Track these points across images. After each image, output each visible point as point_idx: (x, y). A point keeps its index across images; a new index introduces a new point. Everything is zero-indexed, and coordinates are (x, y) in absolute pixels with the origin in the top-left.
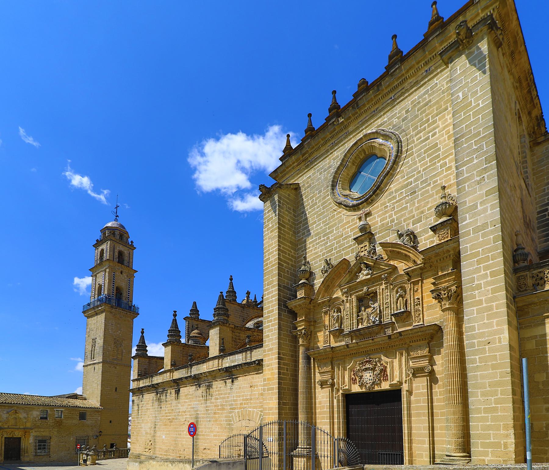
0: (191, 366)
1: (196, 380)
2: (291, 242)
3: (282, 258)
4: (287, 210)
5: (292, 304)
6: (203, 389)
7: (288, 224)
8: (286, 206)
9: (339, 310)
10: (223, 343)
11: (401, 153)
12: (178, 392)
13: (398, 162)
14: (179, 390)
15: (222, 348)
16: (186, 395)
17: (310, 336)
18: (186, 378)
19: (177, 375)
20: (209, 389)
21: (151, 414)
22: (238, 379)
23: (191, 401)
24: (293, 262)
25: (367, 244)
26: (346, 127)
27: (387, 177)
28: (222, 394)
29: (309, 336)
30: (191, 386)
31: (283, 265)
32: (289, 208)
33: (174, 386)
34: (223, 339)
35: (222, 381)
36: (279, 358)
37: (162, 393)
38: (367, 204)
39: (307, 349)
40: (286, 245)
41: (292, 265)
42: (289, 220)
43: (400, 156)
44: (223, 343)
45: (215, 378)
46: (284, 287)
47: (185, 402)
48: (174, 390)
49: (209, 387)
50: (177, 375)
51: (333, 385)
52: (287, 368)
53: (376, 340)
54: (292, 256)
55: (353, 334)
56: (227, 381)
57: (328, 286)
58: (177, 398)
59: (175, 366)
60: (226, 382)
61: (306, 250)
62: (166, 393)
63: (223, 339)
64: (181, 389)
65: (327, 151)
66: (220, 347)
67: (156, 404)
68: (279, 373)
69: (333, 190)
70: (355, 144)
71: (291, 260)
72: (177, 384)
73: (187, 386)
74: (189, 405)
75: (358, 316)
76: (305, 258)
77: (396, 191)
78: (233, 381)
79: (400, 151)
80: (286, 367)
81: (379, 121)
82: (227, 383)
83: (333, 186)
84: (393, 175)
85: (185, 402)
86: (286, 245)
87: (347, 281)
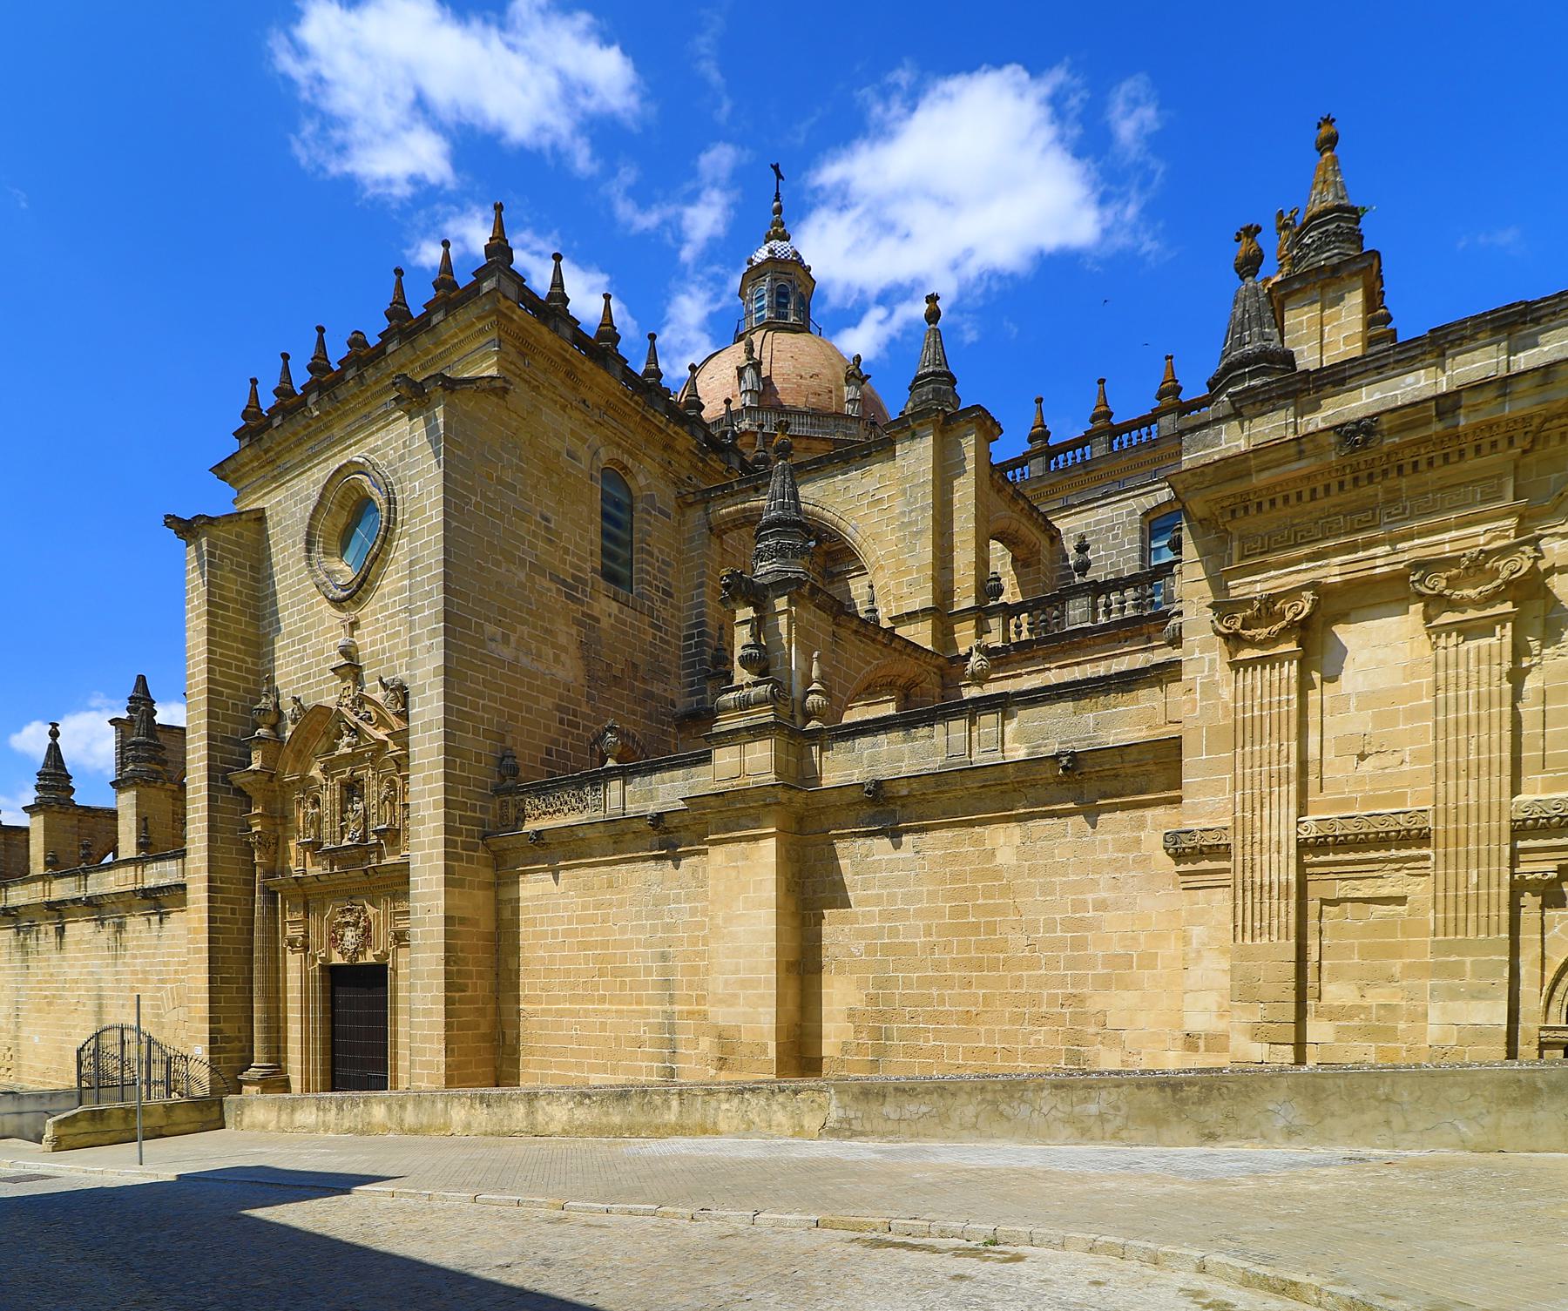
0: (86, 873)
1: (95, 907)
2: (244, 641)
3: (218, 677)
4: (232, 571)
5: (239, 778)
6: (108, 931)
7: (236, 601)
8: (232, 561)
9: (316, 802)
10: (146, 828)
11: (395, 524)
12: (61, 932)
13: (391, 542)
14: (63, 929)
15: (142, 840)
16: (78, 943)
17: (275, 845)
18: (74, 901)
19: (62, 889)
20: (121, 934)
21: (8, 982)
22: (171, 916)
23: (86, 958)
24: (249, 683)
25: (351, 684)
26: (328, 427)
27: (376, 564)
28: (142, 947)
29: (273, 847)
30: (88, 921)
31: (221, 693)
32: (239, 565)
33: (52, 917)
34: (145, 819)
35: (143, 918)
36: (210, 889)
37: (28, 932)
38: (354, 603)
39: (270, 873)
40: (231, 648)
41: (247, 691)
42: (239, 593)
43: (394, 530)
44: (146, 828)
45: (129, 909)
46: (225, 740)
47: (76, 959)
48: (53, 927)
49: (120, 927)
50: (62, 889)
51: (306, 948)
52: (232, 909)
53: (351, 874)
54: (248, 671)
55: (334, 855)
56: (151, 917)
57: (300, 751)
58: (60, 946)
59: (57, 866)
60: (149, 920)
61: (273, 660)
62: (38, 932)
63: (145, 819)
64: (68, 926)
65: (302, 463)
66: (138, 837)
67: (17, 956)
68: (211, 920)
69: (309, 551)
70: (338, 471)
71: (246, 680)
72: (58, 911)
73: (77, 921)
74: (84, 966)
75: (343, 820)
76: (271, 680)
77: (390, 595)
78: (161, 920)
79: (392, 519)
80: (230, 906)
81: (372, 442)
82: (152, 922)
83: (310, 544)
84: (384, 561)
85: (76, 959)
86: (231, 648)
87: (325, 748)
